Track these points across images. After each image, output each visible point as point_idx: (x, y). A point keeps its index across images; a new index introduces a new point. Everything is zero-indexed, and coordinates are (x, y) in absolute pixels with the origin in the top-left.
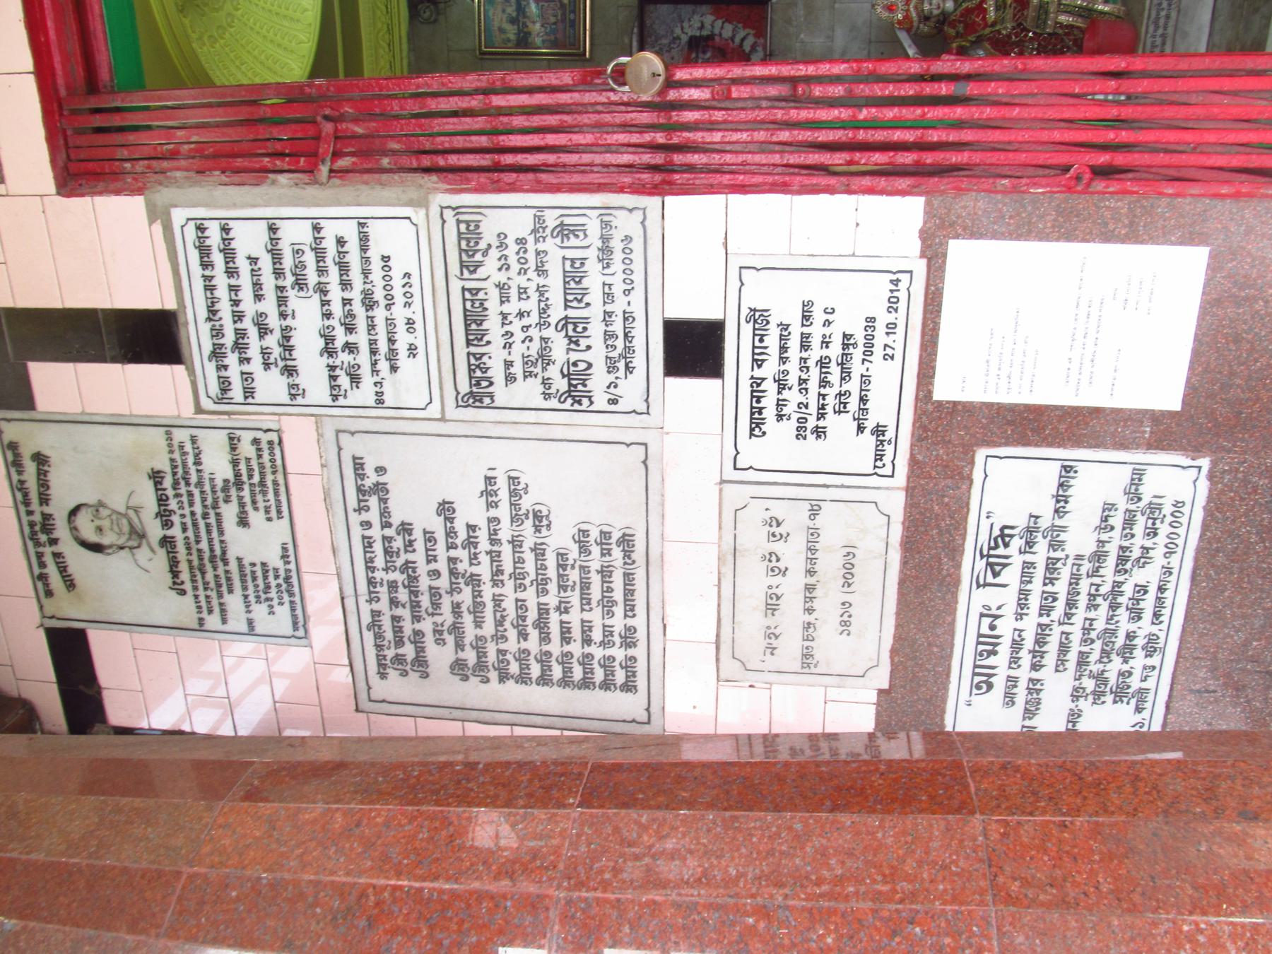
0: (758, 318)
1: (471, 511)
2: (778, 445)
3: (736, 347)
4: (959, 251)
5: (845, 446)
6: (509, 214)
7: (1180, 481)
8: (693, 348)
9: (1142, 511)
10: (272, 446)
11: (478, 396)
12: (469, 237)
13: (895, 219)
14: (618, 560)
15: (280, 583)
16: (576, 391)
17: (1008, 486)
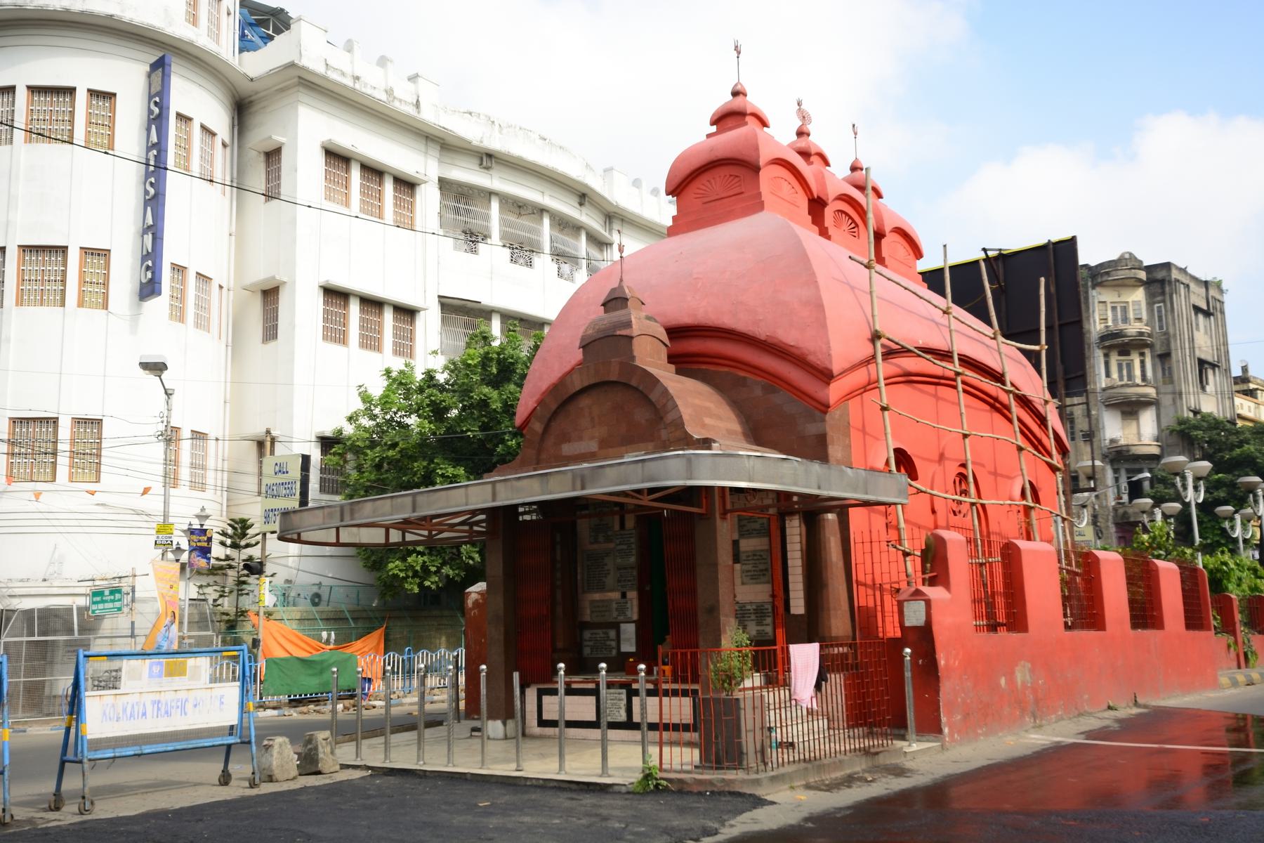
2: (614, 606)
5: (615, 614)
6: (635, 573)
7: (614, 652)
8: (624, 595)
9: (611, 649)
10: (611, 541)
11: (619, 569)
13: (635, 617)
14: (602, 588)
15: (596, 542)
16: (619, 581)
17: (612, 634)
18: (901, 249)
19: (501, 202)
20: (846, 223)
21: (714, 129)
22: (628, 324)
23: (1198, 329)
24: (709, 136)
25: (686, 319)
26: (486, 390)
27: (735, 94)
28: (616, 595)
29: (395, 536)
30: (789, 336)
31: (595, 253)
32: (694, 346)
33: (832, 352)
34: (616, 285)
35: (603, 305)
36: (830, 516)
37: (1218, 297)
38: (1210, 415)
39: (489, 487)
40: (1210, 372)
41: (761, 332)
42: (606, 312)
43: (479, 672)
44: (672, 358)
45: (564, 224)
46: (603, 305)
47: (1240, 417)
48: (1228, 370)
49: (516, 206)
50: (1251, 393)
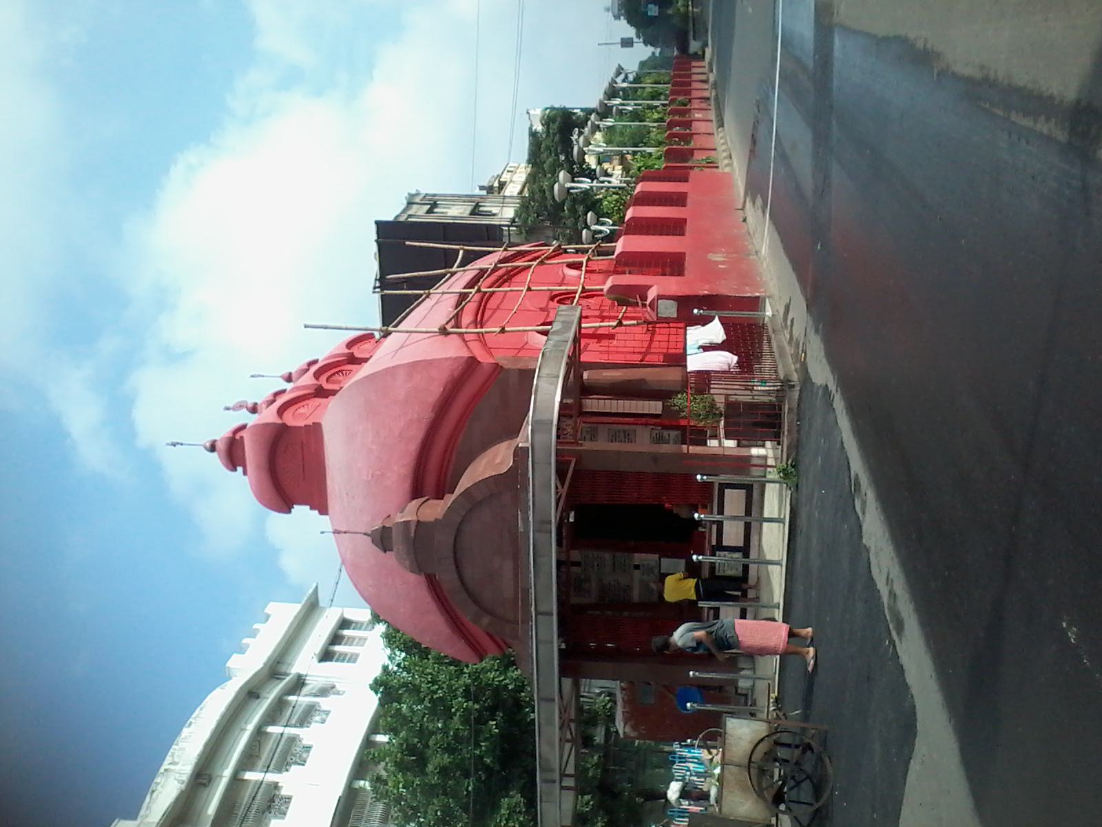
0: (643, 565)
1: (613, 583)
2: (645, 577)
3: (641, 567)
4: (662, 559)
6: (618, 554)
8: (637, 567)
11: (614, 570)
12: (614, 556)
14: (629, 588)
16: (625, 571)
18: (366, 346)
19: (245, 770)
20: (336, 377)
21: (240, 469)
22: (407, 523)
23: (446, 213)
24: (245, 473)
25: (407, 486)
26: (430, 768)
27: (213, 448)
28: (637, 573)
29: (570, 782)
30: (435, 391)
31: (305, 690)
32: (430, 472)
33: (454, 355)
34: (369, 539)
35: (385, 551)
36: (585, 375)
37: (421, 197)
38: (516, 211)
39: (540, 617)
40: (481, 209)
41: (427, 415)
42: (392, 550)
43: (695, 678)
44: (439, 496)
45: (273, 716)
46: (385, 551)
47: (521, 192)
48: (481, 197)
49: (249, 759)
50: (502, 185)
